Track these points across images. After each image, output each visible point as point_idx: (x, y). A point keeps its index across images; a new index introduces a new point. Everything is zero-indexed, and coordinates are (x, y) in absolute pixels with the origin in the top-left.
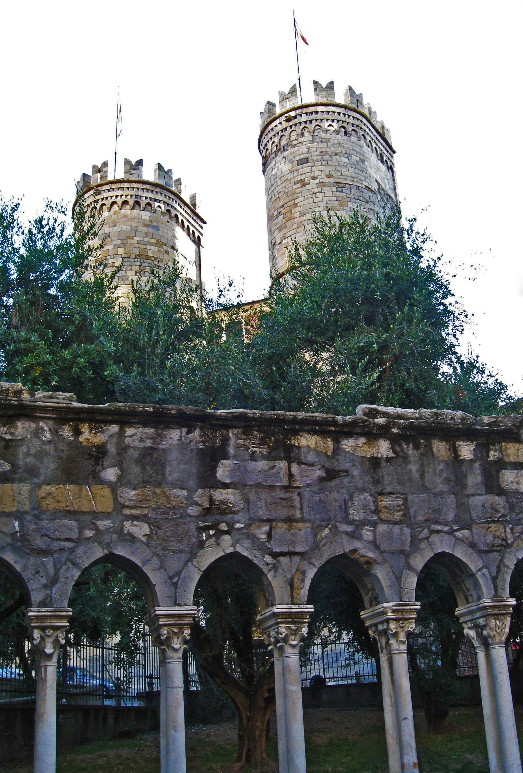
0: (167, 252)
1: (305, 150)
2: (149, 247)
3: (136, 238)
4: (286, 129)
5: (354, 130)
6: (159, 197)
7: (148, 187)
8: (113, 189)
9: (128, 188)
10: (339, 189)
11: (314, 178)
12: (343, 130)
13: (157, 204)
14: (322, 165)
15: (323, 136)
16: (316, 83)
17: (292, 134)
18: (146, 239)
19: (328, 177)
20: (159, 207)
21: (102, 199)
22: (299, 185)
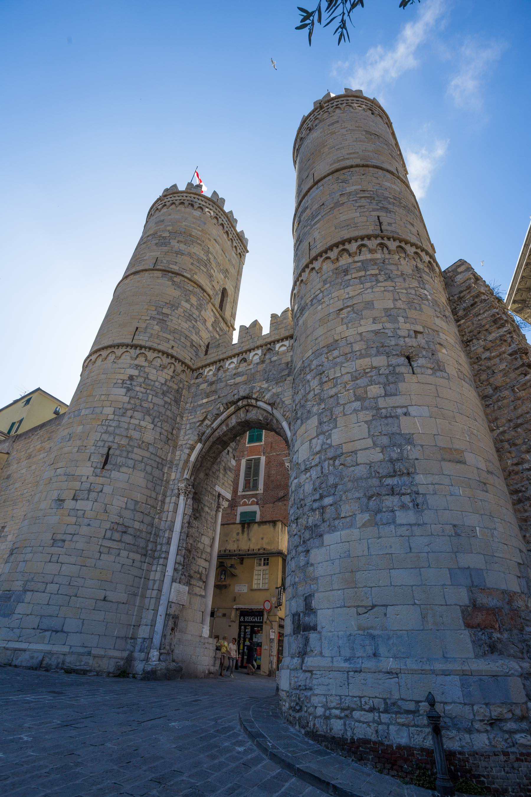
0: (210, 240)
2: (194, 230)
3: (184, 223)
7: (203, 199)
13: (207, 210)
15: (352, 110)
18: (192, 225)
20: (209, 212)
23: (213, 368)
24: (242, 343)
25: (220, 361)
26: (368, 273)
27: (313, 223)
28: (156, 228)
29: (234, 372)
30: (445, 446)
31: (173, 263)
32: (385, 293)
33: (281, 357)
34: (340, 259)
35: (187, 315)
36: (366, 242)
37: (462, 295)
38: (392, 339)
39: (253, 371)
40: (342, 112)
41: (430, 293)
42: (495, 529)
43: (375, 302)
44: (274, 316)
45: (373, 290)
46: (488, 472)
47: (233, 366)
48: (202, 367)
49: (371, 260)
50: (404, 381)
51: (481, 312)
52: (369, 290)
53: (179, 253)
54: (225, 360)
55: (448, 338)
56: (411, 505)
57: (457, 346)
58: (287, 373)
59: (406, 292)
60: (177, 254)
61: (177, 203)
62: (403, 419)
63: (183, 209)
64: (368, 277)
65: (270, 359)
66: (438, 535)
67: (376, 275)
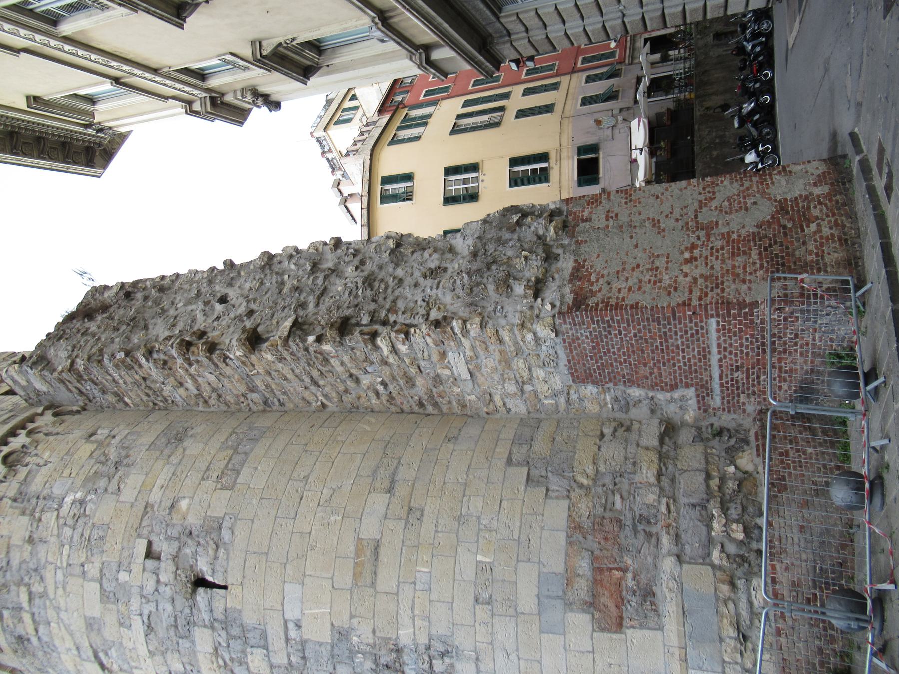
26: (26, 605)
30: (351, 574)
32: (68, 589)
38: (160, 607)
41: (71, 490)
42: (479, 518)
43: (89, 614)
45: (64, 608)
46: (390, 490)
50: (240, 611)
51: (108, 377)
52: (63, 615)
55: (159, 482)
56: (447, 660)
57: (174, 460)
59: (67, 547)
62: (308, 633)
64: (35, 610)
66: (492, 633)
67: (30, 593)
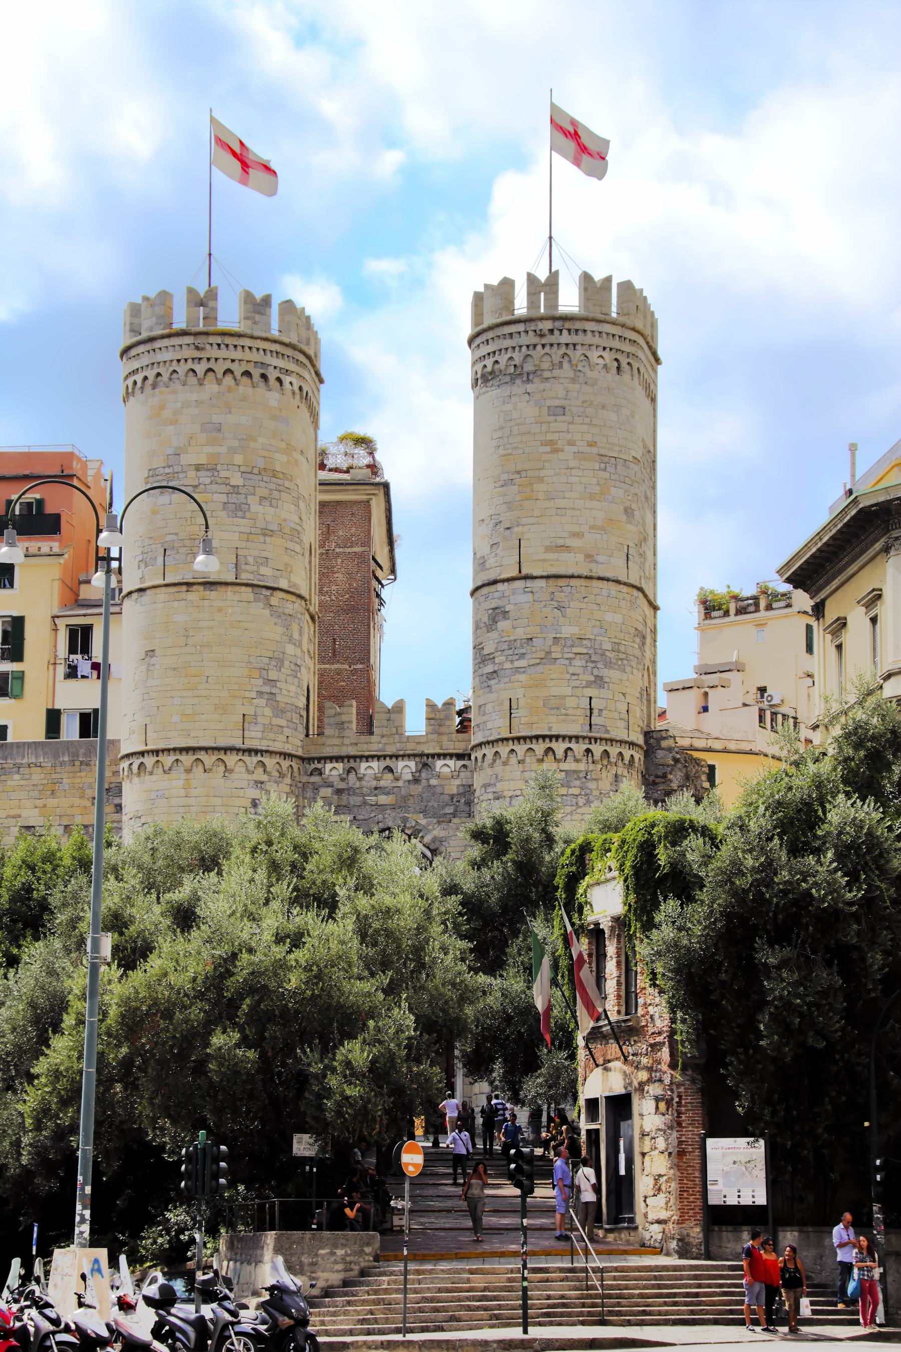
0: (297, 462)
1: (562, 393)
2: (277, 456)
4: (535, 346)
5: (629, 363)
6: (292, 367)
8: (227, 346)
9: (250, 348)
10: (603, 465)
11: (571, 443)
12: (616, 364)
14: (583, 424)
16: (586, 278)
17: (546, 358)
19: (591, 444)
20: (291, 383)
21: (208, 359)
22: (548, 449)
23: (340, 766)
24: (383, 736)
25: (349, 757)
27: (518, 664)
28: (209, 449)
29: (374, 783)
31: (260, 561)
33: (443, 782)
34: (545, 758)
35: (293, 667)
36: (573, 745)
37: (658, 780)
39: (403, 792)
40: (571, 374)
44: (431, 706)
47: (370, 771)
48: (319, 759)
49: (575, 771)
53: (266, 533)
54: (358, 760)
58: (451, 811)
60: (265, 535)
61: (238, 369)
63: (250, 390)
64: (569, 798)
65: (428, 780)
